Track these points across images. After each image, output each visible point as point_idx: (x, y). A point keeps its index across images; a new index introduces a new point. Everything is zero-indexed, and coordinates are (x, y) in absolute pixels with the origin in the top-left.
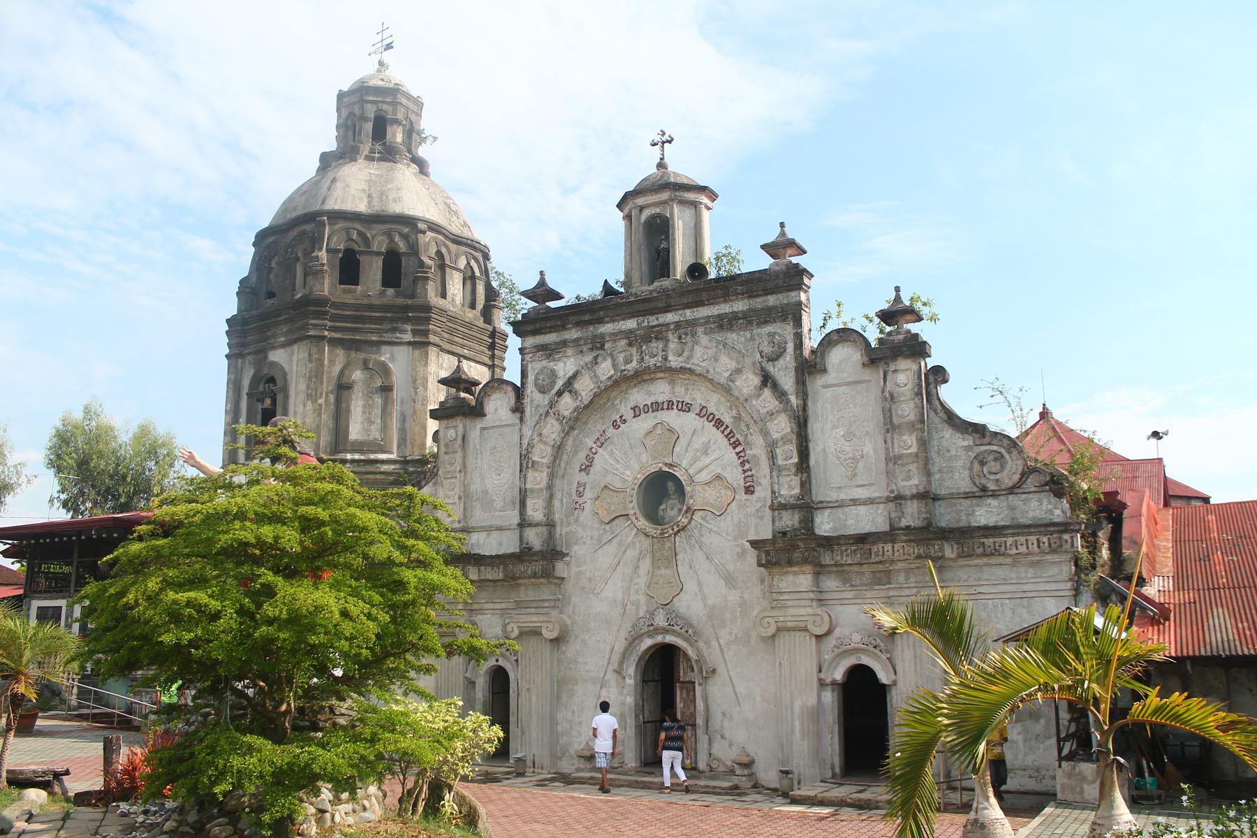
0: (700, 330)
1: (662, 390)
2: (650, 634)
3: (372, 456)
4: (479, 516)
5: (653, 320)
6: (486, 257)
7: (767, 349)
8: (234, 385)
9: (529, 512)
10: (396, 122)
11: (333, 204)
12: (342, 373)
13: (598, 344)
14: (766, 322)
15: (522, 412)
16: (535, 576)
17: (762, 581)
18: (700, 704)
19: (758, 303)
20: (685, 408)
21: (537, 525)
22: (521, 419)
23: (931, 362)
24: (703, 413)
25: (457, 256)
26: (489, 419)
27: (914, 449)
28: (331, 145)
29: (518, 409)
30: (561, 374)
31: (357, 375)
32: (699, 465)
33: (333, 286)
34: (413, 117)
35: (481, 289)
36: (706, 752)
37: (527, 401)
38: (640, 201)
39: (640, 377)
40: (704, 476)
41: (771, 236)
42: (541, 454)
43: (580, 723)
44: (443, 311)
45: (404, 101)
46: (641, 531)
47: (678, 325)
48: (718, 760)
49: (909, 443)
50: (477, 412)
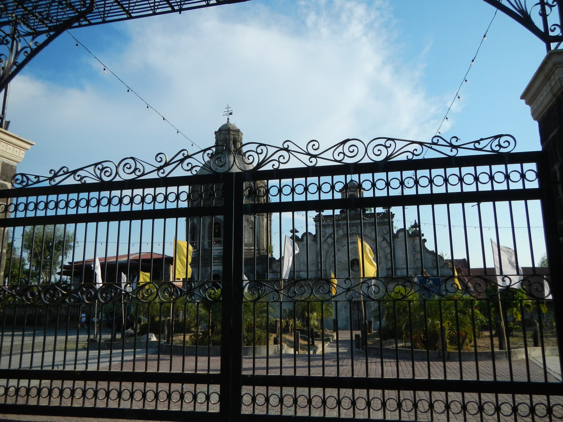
0: (367, 225)
10: (239, 141)
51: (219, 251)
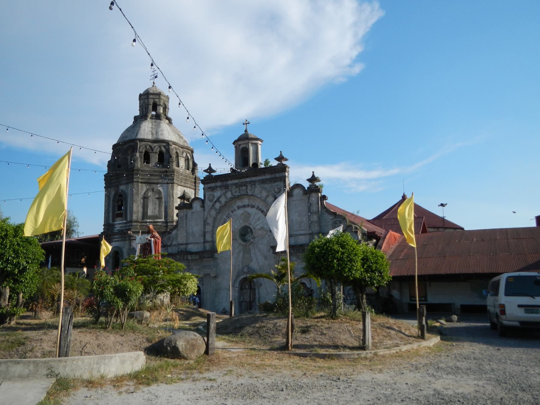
0: (257, 184)
1: (246, 201)
2: (242, 274)
3: (156, 220)
4: (191, 240)
5: (243, 180)
6: (192, 152)
7: (276, 190)
8: (107, 197)
9: (207, 238)
10: (160, 105)
11: (140, 136)
12: (145, 193)
13: (227, 187)
14: (276, 182)
15: (204, 207)
16: (208, 257)
17: (275, 258)
18: (257, 295)
19: (273, 176)
20: (253, 207)
21: (209, 242)
22: (204, 210)
23: (323, 194)
24: (258, 208)
25: (183, 153)
26: (194, 210)
27: (317, 219)
28: (138, 113)
29: (203, 206)
30: (216, 196)
31: (150, 194)
32: (257, 224)
33: (141, 164)
34: (166, 103)
35: (191, 163)
37: (206, 204)
38: (239, 143)
39: (239, 197)
40: (258, 227)
41: (278, 155)
42: (210, 221)
44: (178, 172)
45: (163, 97)
46: (240, 244)
47: (251, 182)
49: (315, 218)
50: (189, 206)
51: (121, 225)
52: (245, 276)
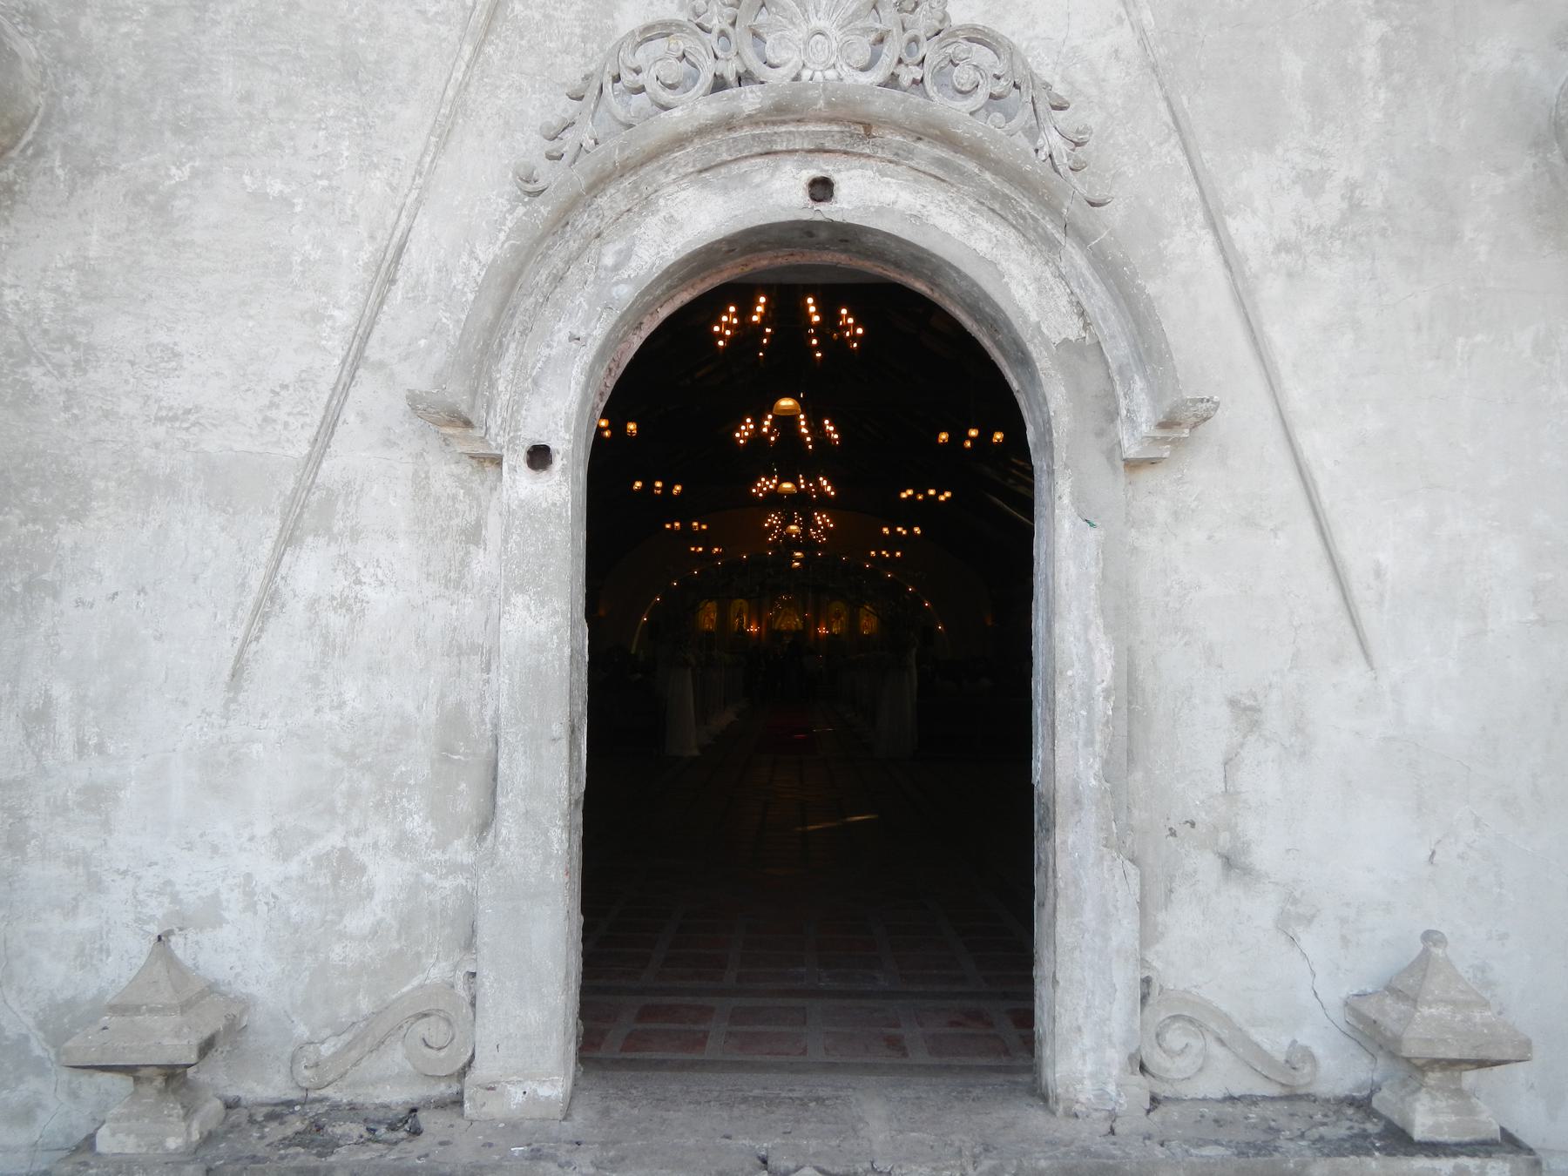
2: (719, 145)
36: (1124, 978)
43: (97, 798)
48: (1194, 1017)
52: (779, 194)
